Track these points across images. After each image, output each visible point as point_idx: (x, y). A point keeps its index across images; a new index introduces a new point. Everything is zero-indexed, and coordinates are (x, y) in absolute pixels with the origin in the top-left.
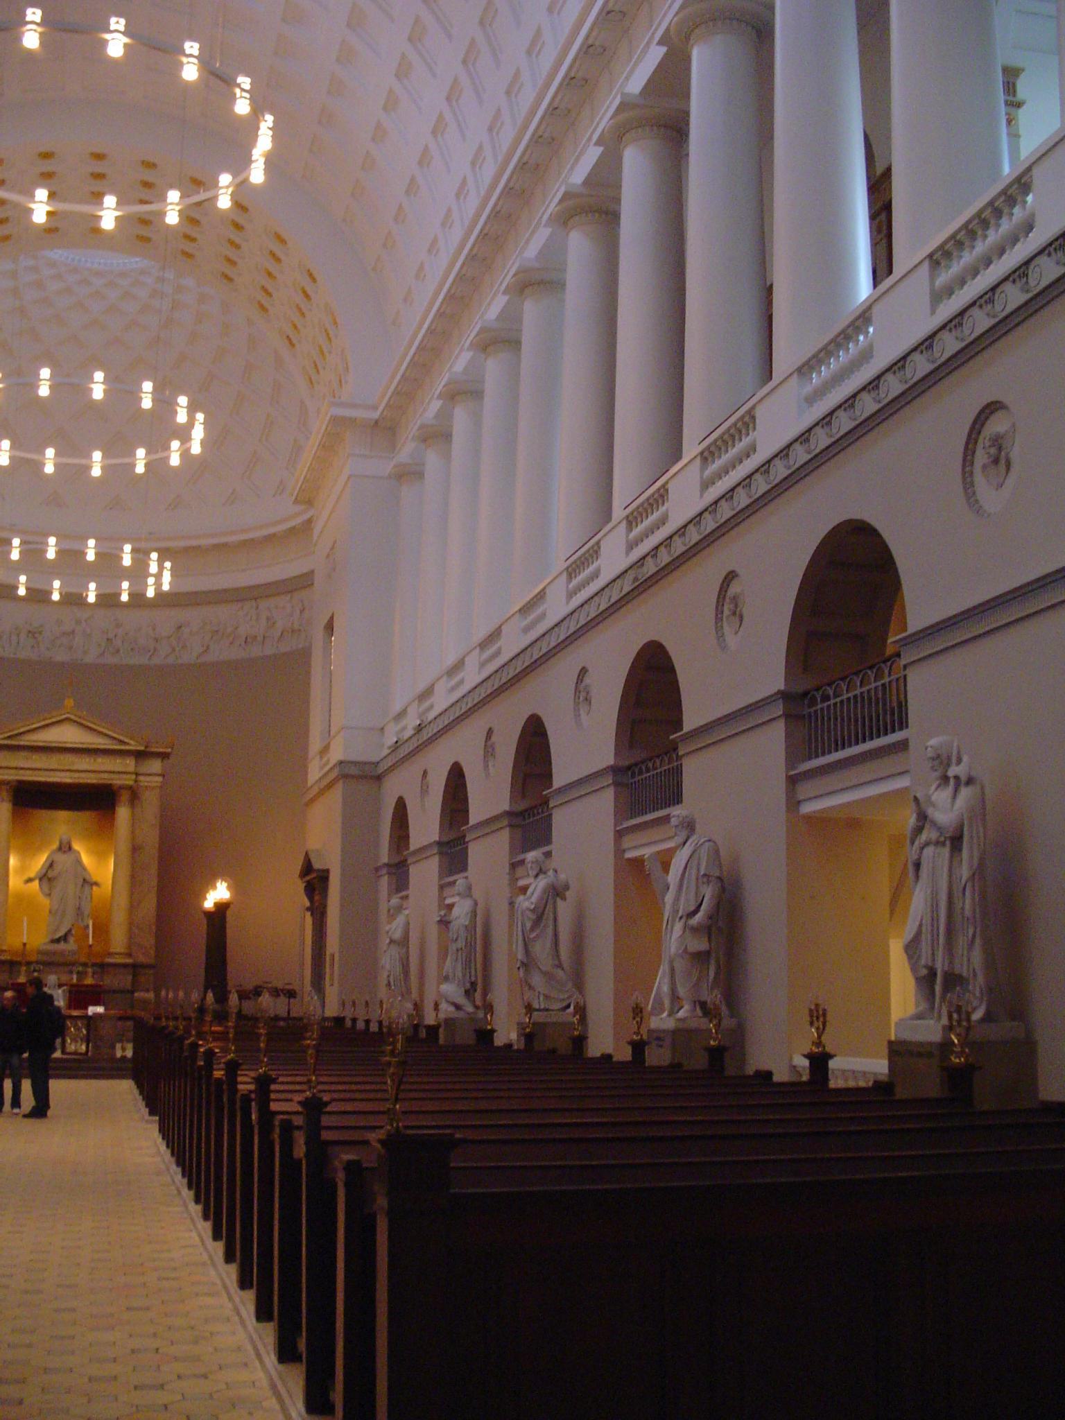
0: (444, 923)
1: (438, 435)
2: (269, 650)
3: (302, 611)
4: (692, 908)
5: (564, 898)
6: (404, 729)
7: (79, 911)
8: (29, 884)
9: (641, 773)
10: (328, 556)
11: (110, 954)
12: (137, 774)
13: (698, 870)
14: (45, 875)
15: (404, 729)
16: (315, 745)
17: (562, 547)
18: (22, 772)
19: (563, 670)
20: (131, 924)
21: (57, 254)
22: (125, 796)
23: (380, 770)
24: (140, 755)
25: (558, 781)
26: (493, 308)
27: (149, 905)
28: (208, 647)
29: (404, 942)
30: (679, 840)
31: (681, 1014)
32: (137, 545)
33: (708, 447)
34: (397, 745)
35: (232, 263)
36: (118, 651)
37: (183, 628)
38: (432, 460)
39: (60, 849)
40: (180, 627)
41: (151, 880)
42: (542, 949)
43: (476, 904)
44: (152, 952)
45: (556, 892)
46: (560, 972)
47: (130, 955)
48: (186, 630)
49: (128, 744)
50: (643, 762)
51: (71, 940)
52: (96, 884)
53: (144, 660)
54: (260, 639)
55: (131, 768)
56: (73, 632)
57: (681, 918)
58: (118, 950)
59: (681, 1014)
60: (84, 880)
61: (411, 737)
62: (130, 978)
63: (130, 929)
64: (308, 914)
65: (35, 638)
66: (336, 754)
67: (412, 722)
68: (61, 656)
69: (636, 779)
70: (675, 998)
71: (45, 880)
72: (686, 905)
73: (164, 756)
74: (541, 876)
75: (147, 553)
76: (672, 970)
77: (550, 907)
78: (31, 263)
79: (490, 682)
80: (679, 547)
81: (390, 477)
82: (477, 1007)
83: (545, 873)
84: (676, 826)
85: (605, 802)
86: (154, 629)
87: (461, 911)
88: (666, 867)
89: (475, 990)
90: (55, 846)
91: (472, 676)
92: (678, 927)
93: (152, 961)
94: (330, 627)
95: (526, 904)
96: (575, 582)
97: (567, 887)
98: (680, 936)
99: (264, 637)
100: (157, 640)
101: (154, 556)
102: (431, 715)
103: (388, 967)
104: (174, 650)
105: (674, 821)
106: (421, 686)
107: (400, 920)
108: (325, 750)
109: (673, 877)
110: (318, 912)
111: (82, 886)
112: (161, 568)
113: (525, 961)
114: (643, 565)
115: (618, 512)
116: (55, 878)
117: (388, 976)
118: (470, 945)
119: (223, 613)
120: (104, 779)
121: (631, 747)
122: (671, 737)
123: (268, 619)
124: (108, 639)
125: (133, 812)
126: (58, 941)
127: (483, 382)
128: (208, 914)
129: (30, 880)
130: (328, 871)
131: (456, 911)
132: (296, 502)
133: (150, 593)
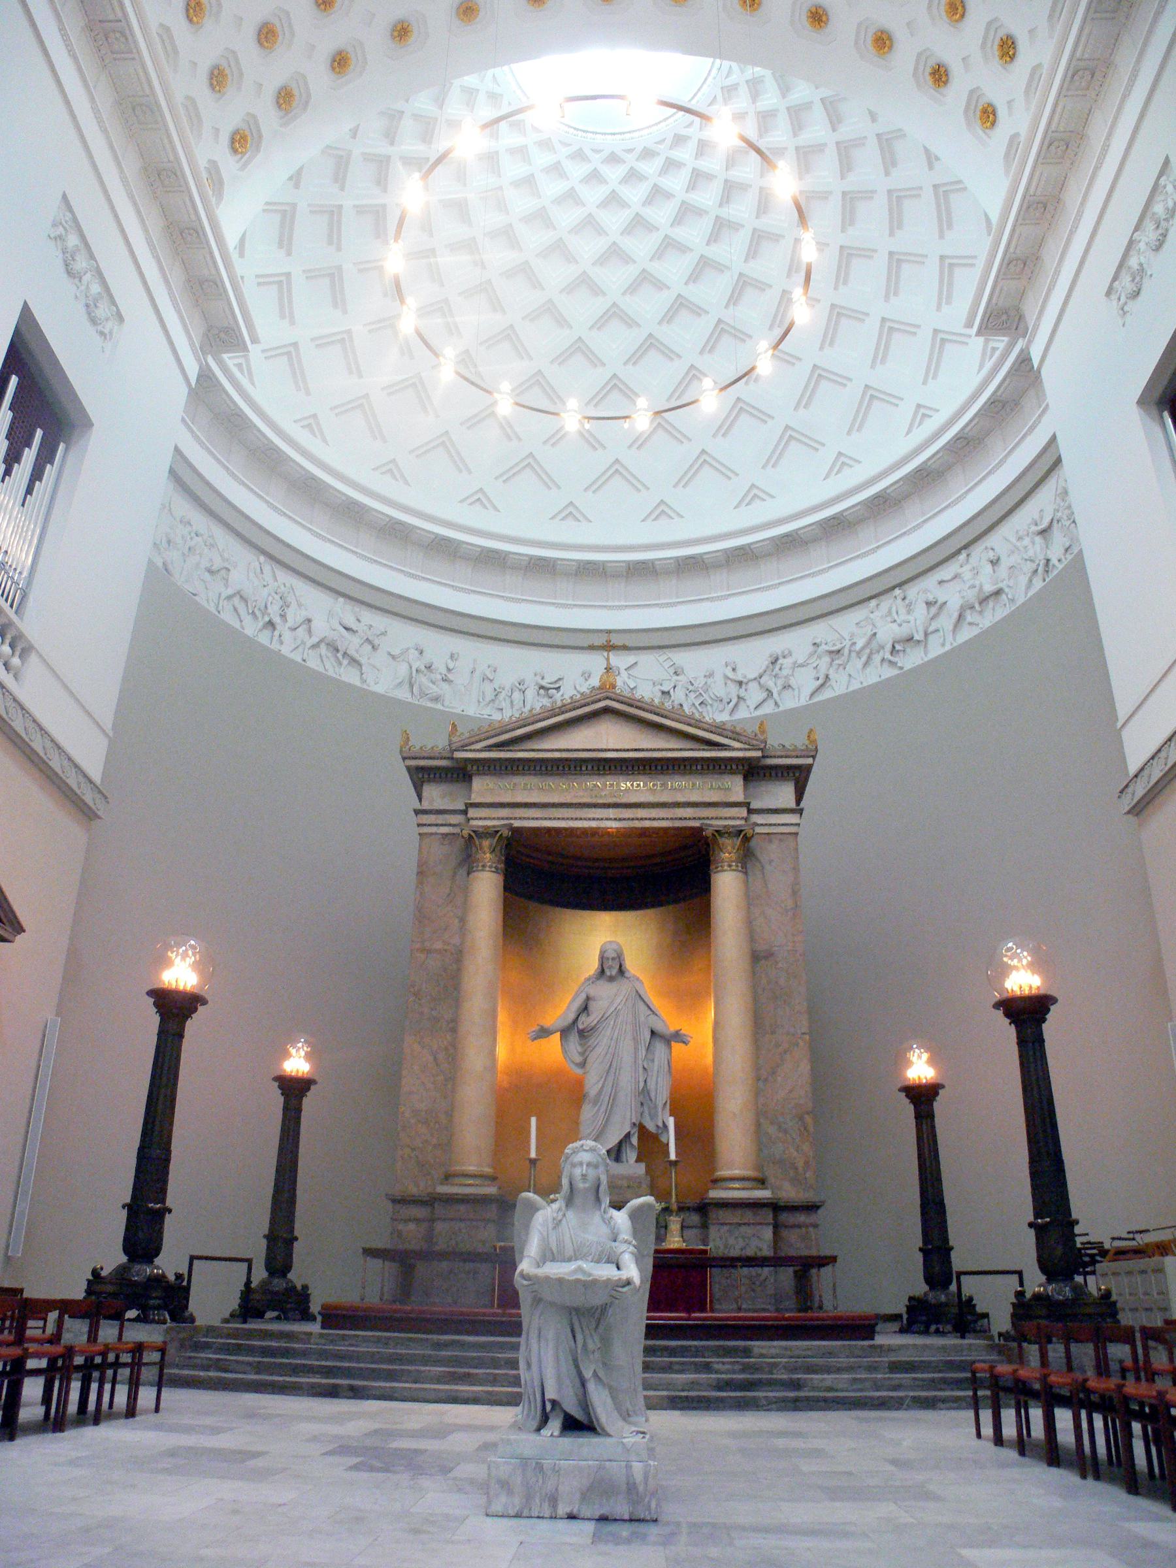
2: (936, 649)
3: (995, 563)
7: (644, 1095)
8: (543, 1042)
12: (750, 811)
22: (727, 852)
28: (827, 676)
37: (780, 661)
39: (602, 972)
40: (774, 662)
47: (762, 1182)
48: (786, 662)
51: (631, 1155)
58: (737, 1172)
60: (653, 1033)
62: (768, 1233)
63: (758, 1125)
71: (574, 1038)
86: (734, 670)
90: (593, 966)
99: (926, 635)
100: (740, 683)
104: (770, 693)
116: (593, 1029)
124: (663, 693)
125: (746, 883)
129: (544, 1033)
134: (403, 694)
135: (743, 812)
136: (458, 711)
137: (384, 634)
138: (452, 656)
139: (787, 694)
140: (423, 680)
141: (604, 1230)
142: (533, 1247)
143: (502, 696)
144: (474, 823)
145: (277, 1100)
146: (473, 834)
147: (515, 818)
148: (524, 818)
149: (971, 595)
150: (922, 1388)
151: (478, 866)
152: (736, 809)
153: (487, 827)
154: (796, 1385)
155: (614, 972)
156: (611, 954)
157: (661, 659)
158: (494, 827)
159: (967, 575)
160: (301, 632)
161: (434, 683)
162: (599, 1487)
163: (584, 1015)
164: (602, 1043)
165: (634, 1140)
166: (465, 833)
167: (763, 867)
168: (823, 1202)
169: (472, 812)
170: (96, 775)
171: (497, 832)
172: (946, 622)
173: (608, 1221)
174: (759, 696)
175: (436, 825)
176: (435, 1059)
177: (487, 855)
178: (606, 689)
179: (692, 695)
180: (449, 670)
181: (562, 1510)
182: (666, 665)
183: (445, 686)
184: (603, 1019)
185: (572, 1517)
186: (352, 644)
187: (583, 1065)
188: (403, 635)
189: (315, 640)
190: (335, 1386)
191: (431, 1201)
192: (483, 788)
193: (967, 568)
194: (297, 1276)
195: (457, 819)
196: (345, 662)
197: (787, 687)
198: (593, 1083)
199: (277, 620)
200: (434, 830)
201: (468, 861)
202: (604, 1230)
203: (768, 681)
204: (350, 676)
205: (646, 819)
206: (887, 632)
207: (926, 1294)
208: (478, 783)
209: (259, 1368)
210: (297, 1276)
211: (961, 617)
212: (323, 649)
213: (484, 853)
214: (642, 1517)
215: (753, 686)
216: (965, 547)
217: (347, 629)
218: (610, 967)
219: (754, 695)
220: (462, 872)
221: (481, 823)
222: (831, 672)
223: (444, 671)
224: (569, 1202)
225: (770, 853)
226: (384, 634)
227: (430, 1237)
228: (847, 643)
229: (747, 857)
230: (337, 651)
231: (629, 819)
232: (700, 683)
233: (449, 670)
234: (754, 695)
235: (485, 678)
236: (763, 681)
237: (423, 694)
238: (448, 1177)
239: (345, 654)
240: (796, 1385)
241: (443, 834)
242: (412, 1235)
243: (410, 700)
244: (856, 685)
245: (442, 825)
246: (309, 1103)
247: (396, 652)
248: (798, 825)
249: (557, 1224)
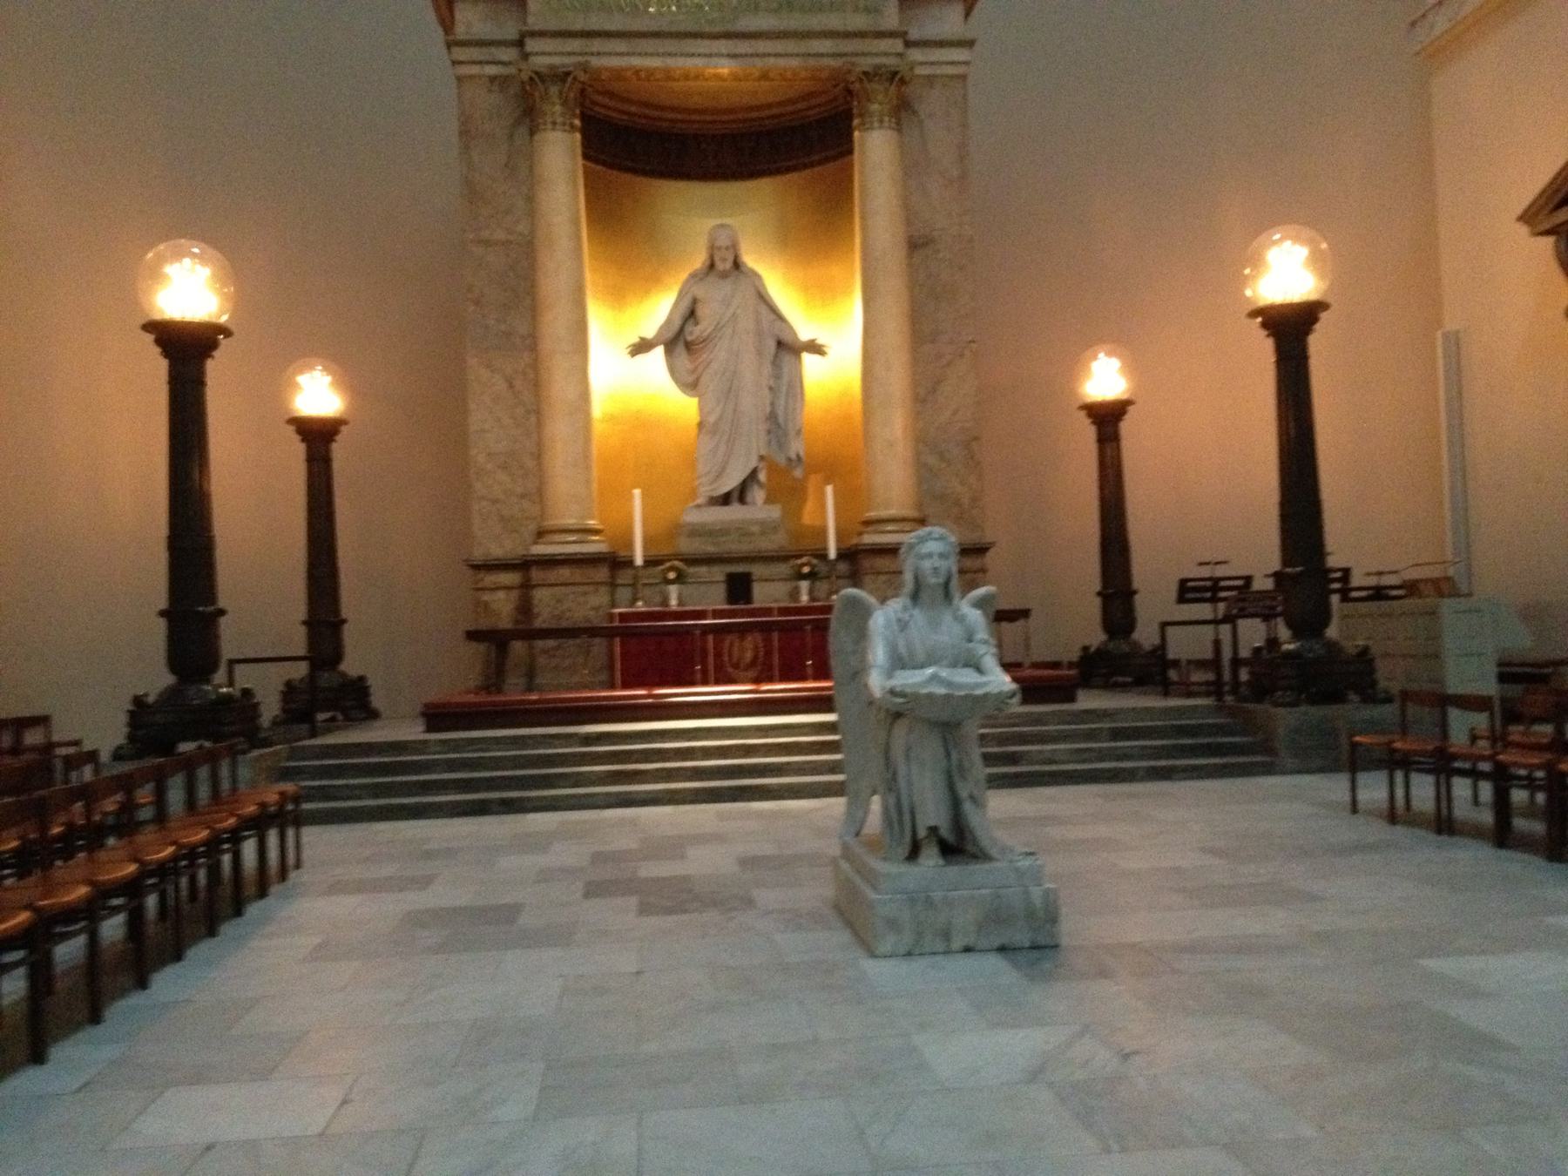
8: (641, 358)
14: (681, 330)
51: (758, 495)
52: (815, 348)
71: (680, 348)
90: (699, 261)
111: (776, 356)
126: (725, 500)
135: (897, 45)
141: (957, 630)
142: (878, 654)
145: (300, 449)
146: (533, 75)
147: (592, 54)
148: (605, 54)
150: (1150, 757)
151: (545, 124)
152: (890, 41)
153: (552, 67)
154: (1013, 759)
155: (728, 265)
156: (723, 241)
158: (564, 66)
162: (996, 916)
163: (691, 321)
164: (719, 355)
166: (525, 76)
167: (921, 122)
168: (992, 544)
169: (532, 45)
171: (568, 74)
173: (960, 619)
175: (480, 63)
176: (511, 386)
181: (957, 944)
184: (718, 328)
185: (968, 950)
190: (483, 801)
191: (525, 565)
194: (351, 665)
195: (508, 54)
200: (475, 70)
201: (529, 116)
202: (957, 630)
205: (769, 55)
207: (1105, 643)
209: (377, 791)
210: (351, 665)
213: (554, 104)
214: (1043, 943)
218: (724, 260)
220: (523, 131)
221: (547, 60)
224: (915, 597)
225: (931, 103)
227: (525, 608)
229: (902, 110)
231: (746, 55)
238: (541, 534)
240: (1013, 759)
241: (489, 77)
242: (502, 606)
245: (488, 63)
248: (966, 63)
249: (903, 625)
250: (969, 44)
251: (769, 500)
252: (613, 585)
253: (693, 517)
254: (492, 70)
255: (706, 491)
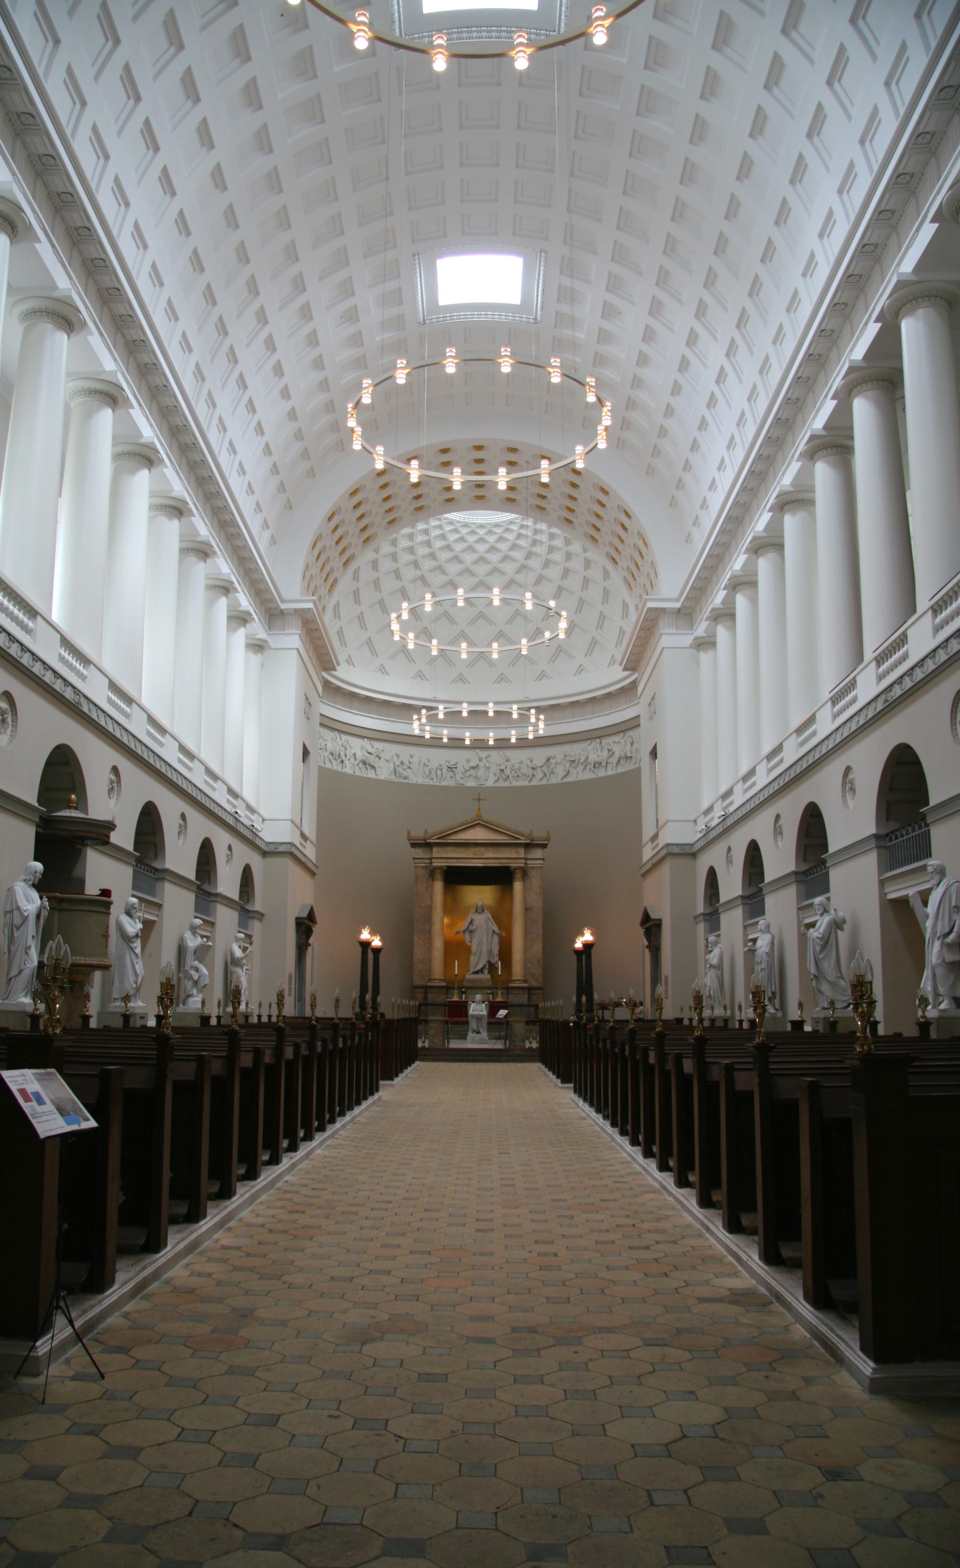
0: (752, 952)
1: (726, 615)
2: (610, 772)
3: (632, 744)
4: (947, 930)
5: (842, 929)
6: (712, 819)
7: (490, 951)
9: (896, 838)
10: (650, 704)
11: (512, 981)
13: (950, 901)
15: (712, 819)
16: (648, 832)
17: (828, 682)
18: (449, 860)
19: (835, 770)
20: (526, 960)
21: (454, 516)
22: (518, 875)
23: (696, 847)
24: (528, 846)
25: (833, 847)
26: (761, 522)
27: (537, 948)
28: (569, 772)
29: (719, 967)
30: (934, 882)
31: (942, 1006)
32: (521, 705)
33: (937, 603)
34: (709, 830)
35: (571, 510)
36: (508, 777)
37: (551, 760)
38: (722, 633)
40: (548, 760)
41: (538, 930)
42: (828, 967)
43: (773, 937)
44: (541, 979)
45: (837, 925)
46: (842, 982)
47: (525, 981)
48: (553, 761)
49: (519, 839)
50: (898, 830)
53: (526, 783)
54: (604, 764)
55: (522, 855)
56: (478, 765)
57: (939, 937)
58: (518, 978)
59: (942, 1006)
61: (717, 825)
62: (526, 997)
64: (647, 951)
65: (453, 772)
66: (662, 841)
67: (718, 813)
68: (471, 783)
69: (893, 843)
70: (937, 995)
71: (467, 933)
72: (942, 927)
73: (544, 846)
74: (826, 914)
75: (529, 709)
76: (934, 975)
77: (833, 935)
78: (437, 523)
79: (777, 782)
80: (919, 675)
81: (691, 647)
82: (776, 1009)
83: (828, 912)
84: (932, 873)
85: (870, 862)
87: (763, 943)
88: (925, 903)
89: (775, 998)
90: (474, 910)
91: (762, 779)
92: (937, 945)
93: (541, 985)
94: (654, 753)
95: (816, 934)
96: (837, 707)
97: (844, 921)
98: (939, 951)
99: (607, 763)
100: (534, 768)
101: (533, 711)
102: (731, 809)
103: (709, 984)
104: (545, 775)
105: (930, 869)
106: (723, 789)
107: (716, 951)
108: (655, 837)
109: (931, 909)
110: (655, 949)
112: (538, 719)
113: (816, 974)
114: (891, 690)
115: (869, 655)
117: (710, 990)
118: (770, 966)
119: (577, 750)
120: (504, 863)
121: (888, 820)
122: (921, 811)
123: (609, 750)
126: (477, 972)
127: (757, 575)
128: (578, 953)
130: (660, 920)
131: (759, 943)
132: (625, 669)
133: (531, 736)
134: (393, 777)
135: (524, 861)
136: (414, 782)
137: (383, 751)
138: (411, 756)
139: (552, 776)
140: (400, 769)
142: (471, 1009)
143: (433, 772)
144: (434, 864)
149: (623, 754)
157: (501, 753)
159: (622, 741)
160: (352, 760)
161: (404, 770)
165: (487, 966)
169: (433, 860)
170: (314, 861)
172: (614, 760)
174: (541, 775)
177: (439, 876)
178: (479, 817)
179: (513, 772)
180: (410, 763)
182: (503, 756)
183: (409, 770)
186: (372, 760)
187: (471, 942)
188: (389, 750)
189: (357, 762)
191: (426, 988)
192: (437, 852)
193: (623, 740)
195: (428, 861)
196: (369, 768)
197: (552, 772)
198: (474, 949)
199: (344, 758)
203: (545, 769)
204: (371, 774)
206: (593, 757)
208: (435, 850)
211: (619, 761)
212: (361, 765)
215: (539, 770)
216: (623, 731)
217: (369, 753)
219: (539, 774)
222: (571, 770)
223: (408, 763)
225: (534, 874)
226: (383, 751)
228: (577, 758)
230: (366, 764)
232: (517, 766)
233: (410, 763)
234: (539, 774)
235: (425, 765)
236: (543, 768)
237: (400, 776)
238: (430, 980)
239: (369, 765)
243: (396, 780)
244: (579, 778)
246: (382, 956)
247: (388, 758)
250: (543, 859)
251: (489, 973)
252: (447, 993)
253: (467, 977)
254: (423, 865)
255: (472, 970)
